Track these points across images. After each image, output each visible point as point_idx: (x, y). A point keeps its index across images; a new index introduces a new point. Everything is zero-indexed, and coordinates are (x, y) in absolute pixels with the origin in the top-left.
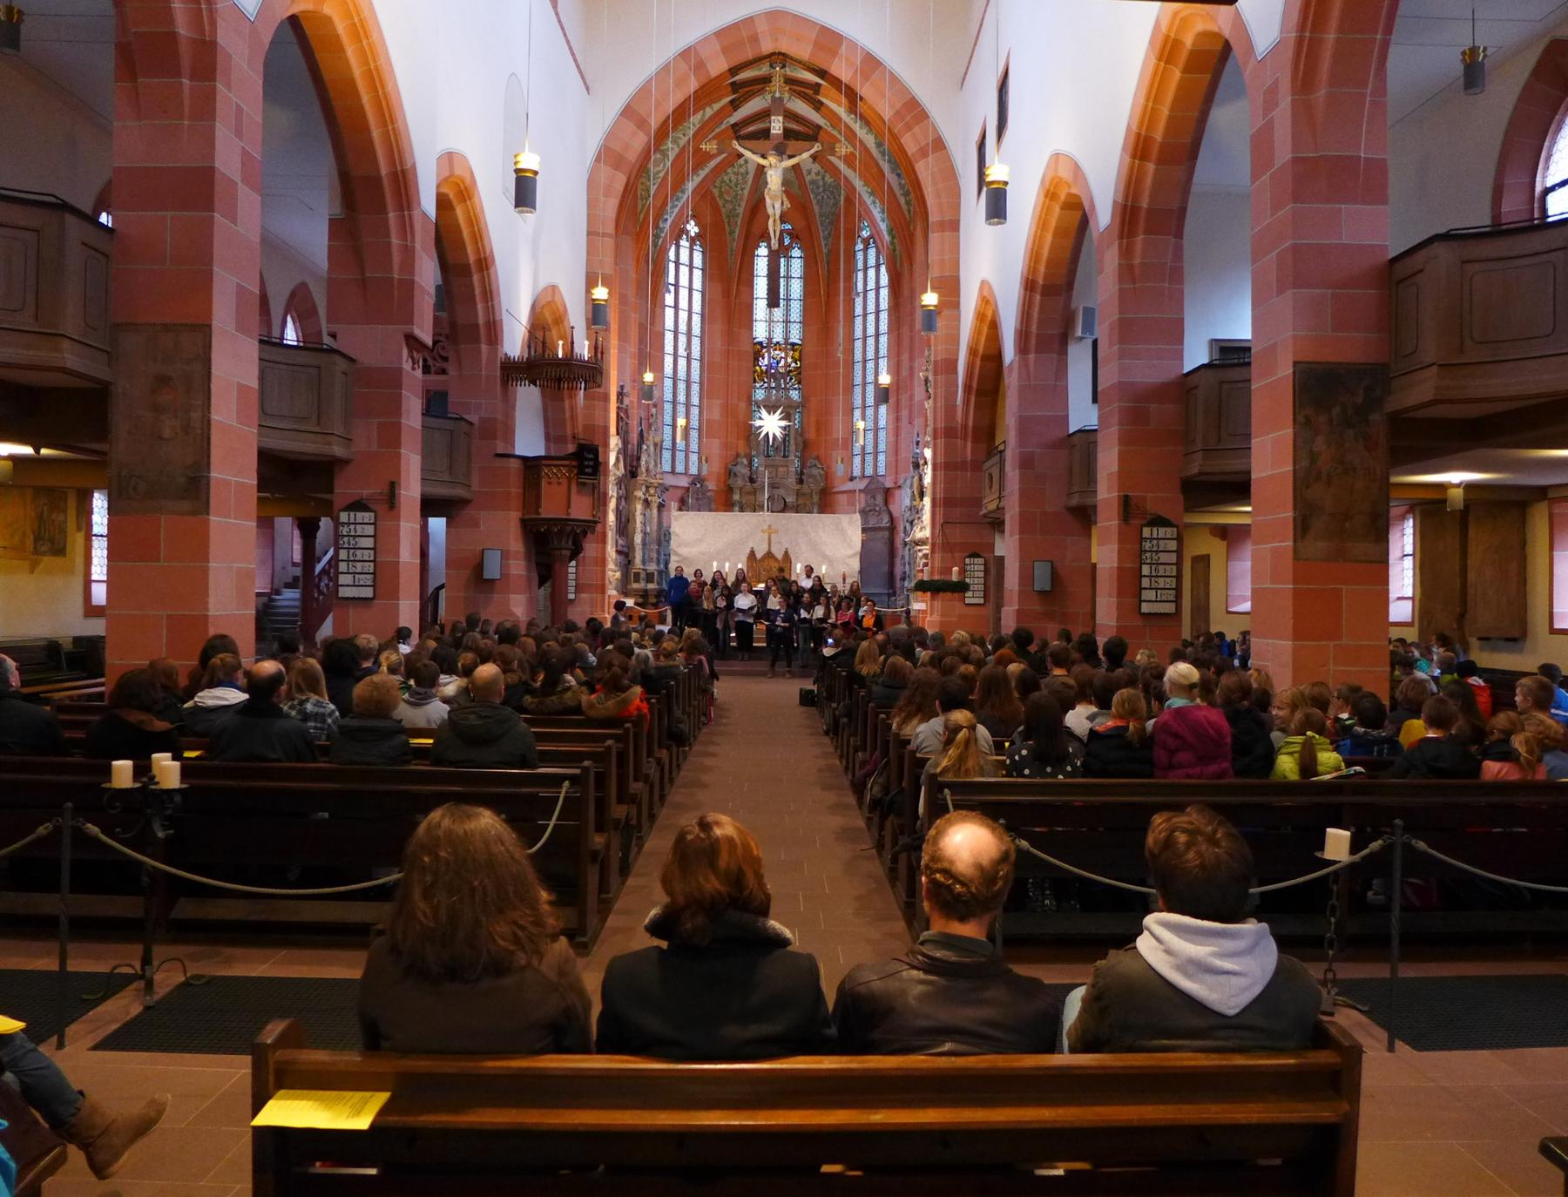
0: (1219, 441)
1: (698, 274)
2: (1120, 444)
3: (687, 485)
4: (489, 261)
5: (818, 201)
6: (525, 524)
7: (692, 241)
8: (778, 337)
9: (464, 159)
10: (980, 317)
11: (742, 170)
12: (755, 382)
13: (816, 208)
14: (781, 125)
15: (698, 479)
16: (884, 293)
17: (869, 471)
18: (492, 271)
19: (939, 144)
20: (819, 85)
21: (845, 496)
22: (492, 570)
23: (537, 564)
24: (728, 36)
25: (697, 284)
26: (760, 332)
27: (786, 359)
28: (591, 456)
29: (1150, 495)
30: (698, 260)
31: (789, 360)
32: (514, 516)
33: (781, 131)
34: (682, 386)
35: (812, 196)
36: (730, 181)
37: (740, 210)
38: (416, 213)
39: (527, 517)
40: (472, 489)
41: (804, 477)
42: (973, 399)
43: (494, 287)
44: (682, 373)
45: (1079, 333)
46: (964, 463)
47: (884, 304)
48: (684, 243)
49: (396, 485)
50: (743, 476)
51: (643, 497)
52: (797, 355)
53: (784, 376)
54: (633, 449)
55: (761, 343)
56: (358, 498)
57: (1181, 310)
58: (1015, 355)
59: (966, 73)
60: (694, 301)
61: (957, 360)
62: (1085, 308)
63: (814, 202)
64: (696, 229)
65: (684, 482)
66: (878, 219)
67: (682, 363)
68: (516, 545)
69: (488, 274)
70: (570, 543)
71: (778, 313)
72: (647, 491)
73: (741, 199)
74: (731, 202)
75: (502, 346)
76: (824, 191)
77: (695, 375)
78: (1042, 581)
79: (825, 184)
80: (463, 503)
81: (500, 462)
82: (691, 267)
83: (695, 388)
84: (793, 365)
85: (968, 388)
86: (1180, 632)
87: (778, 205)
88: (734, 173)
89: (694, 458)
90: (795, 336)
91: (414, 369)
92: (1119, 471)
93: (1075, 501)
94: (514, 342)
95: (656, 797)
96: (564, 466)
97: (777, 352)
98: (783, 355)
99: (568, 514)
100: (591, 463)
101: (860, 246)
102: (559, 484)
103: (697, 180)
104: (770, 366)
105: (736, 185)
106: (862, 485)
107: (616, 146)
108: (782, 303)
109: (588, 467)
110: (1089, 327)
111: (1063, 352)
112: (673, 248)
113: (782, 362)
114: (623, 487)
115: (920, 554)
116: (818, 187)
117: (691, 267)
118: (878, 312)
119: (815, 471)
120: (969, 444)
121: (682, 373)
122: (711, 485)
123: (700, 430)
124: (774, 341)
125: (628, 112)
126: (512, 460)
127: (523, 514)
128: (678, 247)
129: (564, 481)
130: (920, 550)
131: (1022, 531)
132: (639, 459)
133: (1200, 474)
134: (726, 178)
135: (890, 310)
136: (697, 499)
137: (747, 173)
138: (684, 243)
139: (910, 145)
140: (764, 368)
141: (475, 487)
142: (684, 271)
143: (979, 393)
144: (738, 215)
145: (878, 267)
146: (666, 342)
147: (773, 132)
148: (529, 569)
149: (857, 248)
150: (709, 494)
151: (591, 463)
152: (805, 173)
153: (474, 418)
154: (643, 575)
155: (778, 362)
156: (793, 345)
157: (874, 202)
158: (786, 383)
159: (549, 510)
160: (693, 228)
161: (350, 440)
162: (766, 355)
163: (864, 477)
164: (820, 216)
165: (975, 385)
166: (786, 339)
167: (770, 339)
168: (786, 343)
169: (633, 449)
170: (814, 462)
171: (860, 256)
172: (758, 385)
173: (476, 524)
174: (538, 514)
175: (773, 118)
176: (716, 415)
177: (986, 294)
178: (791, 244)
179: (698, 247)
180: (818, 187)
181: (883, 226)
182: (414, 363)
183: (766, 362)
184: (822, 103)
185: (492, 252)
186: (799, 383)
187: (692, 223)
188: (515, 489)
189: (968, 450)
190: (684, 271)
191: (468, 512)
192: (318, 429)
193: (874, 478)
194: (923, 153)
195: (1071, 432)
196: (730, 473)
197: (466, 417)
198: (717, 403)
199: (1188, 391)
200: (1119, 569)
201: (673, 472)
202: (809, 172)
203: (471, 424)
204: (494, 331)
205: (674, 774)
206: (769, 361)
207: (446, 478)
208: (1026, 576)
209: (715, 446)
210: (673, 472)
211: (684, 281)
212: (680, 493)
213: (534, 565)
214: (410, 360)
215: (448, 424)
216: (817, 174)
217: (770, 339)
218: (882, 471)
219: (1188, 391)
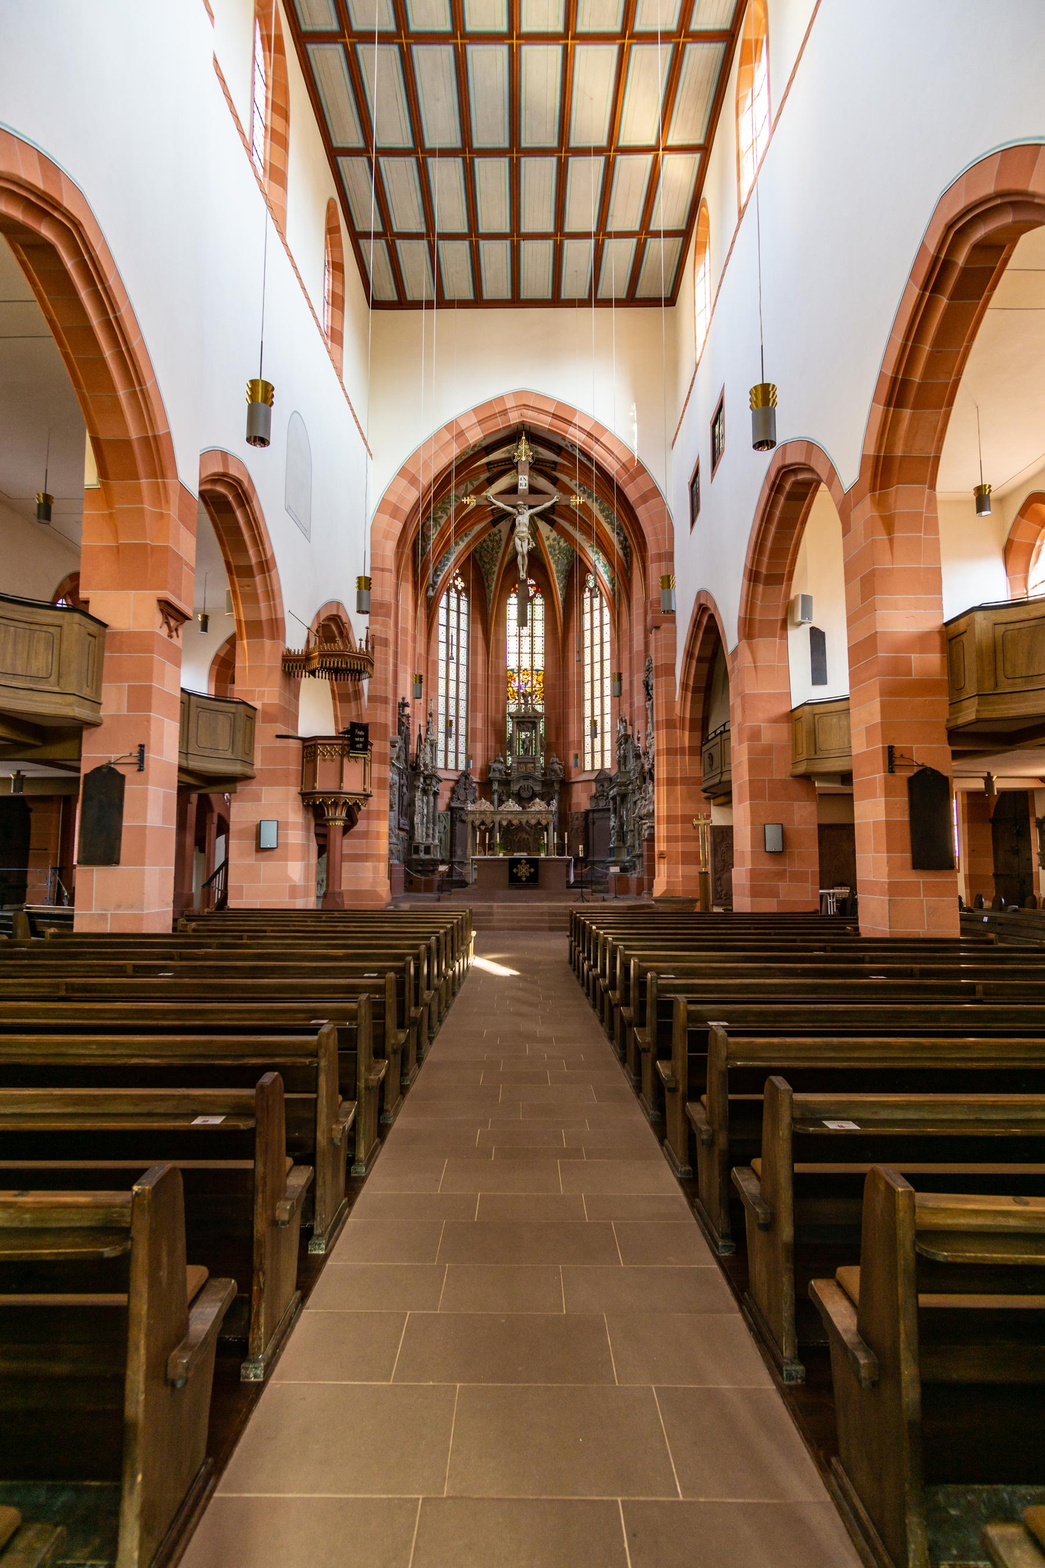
0: (997, 685)
1: (464, 618)
2: (881, 695)
3: (456, 778)
4: (271, 566)
5: (555, 562)
6: (304, 795)
7: (458, 592)
8: (526, 664)
9: (240, 464)
10: (696, 624)
11: (497, 538)
12: (508, 699)
13: (553, 566)
14: (527, 482)
15: (465, 775)
16: (607, 629)
17: (598, 766)
18: (273, 573)
19: (654, 492)
20: (555, 463)
21: (580, 784)
22: (269, 839)
23: (317, 835)
24: (485, 412)
25: (464, 625)
26: (512, 662)
27: (532, 681)
28: (361, 733)
29: (914, 746)
30: (464, 607)
31: (535, 682)
32: (294, 790)
33: (527, 487)
34: (452, 703)
35: (550, 557)
36: (488, 547)
37: (496, 569)
38: (170, 481)
39: (304, 791)
40: (255, 767)
41: (548, 772)
42: (689, 695)
43: (275, 588)
44: (452, 693)
45: (799, 618)
46: (683, 749)
47: (607, 637)
48: (453, 594)
49: (146, 749)
50: (500, 771)
51: (421, 786)
52: (540, 678)
53: (531, 694)
54: (413, 749)
55: (512, 670)
56: (104, 762)
57: (938, 560)
58: (740, 640)
59: (675, 439)
60: (461, 638)
61: (674, 664)
62: (803, 596)
63: (552, 561)
64: (463, 584)
65: (454, 776)
66: (602, 572)
67: (452, 685)
68: (295, 816)
69: (270, 576)
70: (344, 814)
71: (526, 631)
72: (425, 781)
73: (497, 560)
74: (489, 563)
75: (284, 641)
76: (559, 553)
77: (463, 695)
78: (773, 842)
79: (560, 548)
80: (247, 778)
81: (279, 743)
82: (458, 612)
83: (463, 704)
84: (538, 686)
85: (685, 686)
86: (956, 889)
87: (525, 544)
88: (491, 541)
89: (462, 758)
90: (539, 663)
91: (171, 636)
92: (882, 723)
93: (802, 769)
94: (296, 639)
95: (435, 1017)
96: (336, 744)
97: (525, 676)
98: (530, 678)
99: (341, 788)
100: (362, 740)
101: (587, 594)
102: (332, 760)
103: (462, 545)
104: (519, 687)
105: (492, 550)
106: (593, 776)
107: (393, 499)
108: (529, 623)
109: (359, 742)
110: (807, 613)
111: (784, 637)
112: (444, 598)
113: (529, 684)
114: (404, 778)
115: (645, 827)
116: (555, 550)
117: (458, 612)
118: (602, 643)
119: (556, 767)
120: (687, 733)
121: (452, 693)
122: (476, 778)
123: (467, 736)
124: (523, 668)
125: (403, 472)
126: (291, 740)
127: (302, 789)
128: (448, 596)
129: (336, 757)
130: (645, 824)
131: (753, 797)
132: (418, 756)
133: (978, 721)
134: (484, 545)
135: (612, 642)
136: (465, 789)
137: (501, 540)
138: (453, 594)
139: (632, 493)
140: (515, 689)
141: (258, 764)
142: (453, 615)
143: (695, 690)
144: (494, 572)
145: (601, 608)
146: (440, 669)
147: (520, 487)
148: (308, 838)
149: (585, 596)
150: (474, 785)
151: (362, 740)
152: (545, 539)
153: (257, 704)
154: (422, 848)
155: (526, 684)
156: (537, 671)
157: (598, 559)
158: (532, 700)
159: (324, 783)
160: (460, 584)
161: (100, 704)
162: (517, 679)
163: (593, 770)
164: (557, 572)
165: (691, 683)
166: (532, 667)
167: (519, 667)
168: (532, 670)
169: (413, 749)
170: (555, 759)
171: (587, 602)
172: (511, 702)
173: (257, 798)
174: (314, 788)
175: (520, 477)
176: (479, 724)
177: (702, 601)
178: (534, 596)
179: (464, 598)
180: (555, 550)
181: (605, 578)
182: (170, 631)
183: (517, 685)
184: (555, 521)
185: (273, 555)
186: (543, 699)
187: (459, 579)
188: (294, 766)
189: (685, 738)
190: (453, 615)
191: (252, 787)
192: (57, 689)
193: (602, 771)
194: (644, 498)
195: (793, 707)
196: (487, 769)
197: (250, 703)
198: (480, 716)
199: (950, 640)
200: (889, 824)
201: (446, 768)
202: (548, 538)
203: (255, 709)
204: (276, 627)
205: (456, 987)
206: (519, 683)
207: (229, 755)
208: (759, 838)
209: (479, 749)
210: (446, 768)
211: (453, 622)
212: (452, 784)
213: (313, 834)
214: (165, 626)
215: (231, 708)
216: (554, 540)
217: (519, 667)
218: (608, 764)
219: (950, 640)
